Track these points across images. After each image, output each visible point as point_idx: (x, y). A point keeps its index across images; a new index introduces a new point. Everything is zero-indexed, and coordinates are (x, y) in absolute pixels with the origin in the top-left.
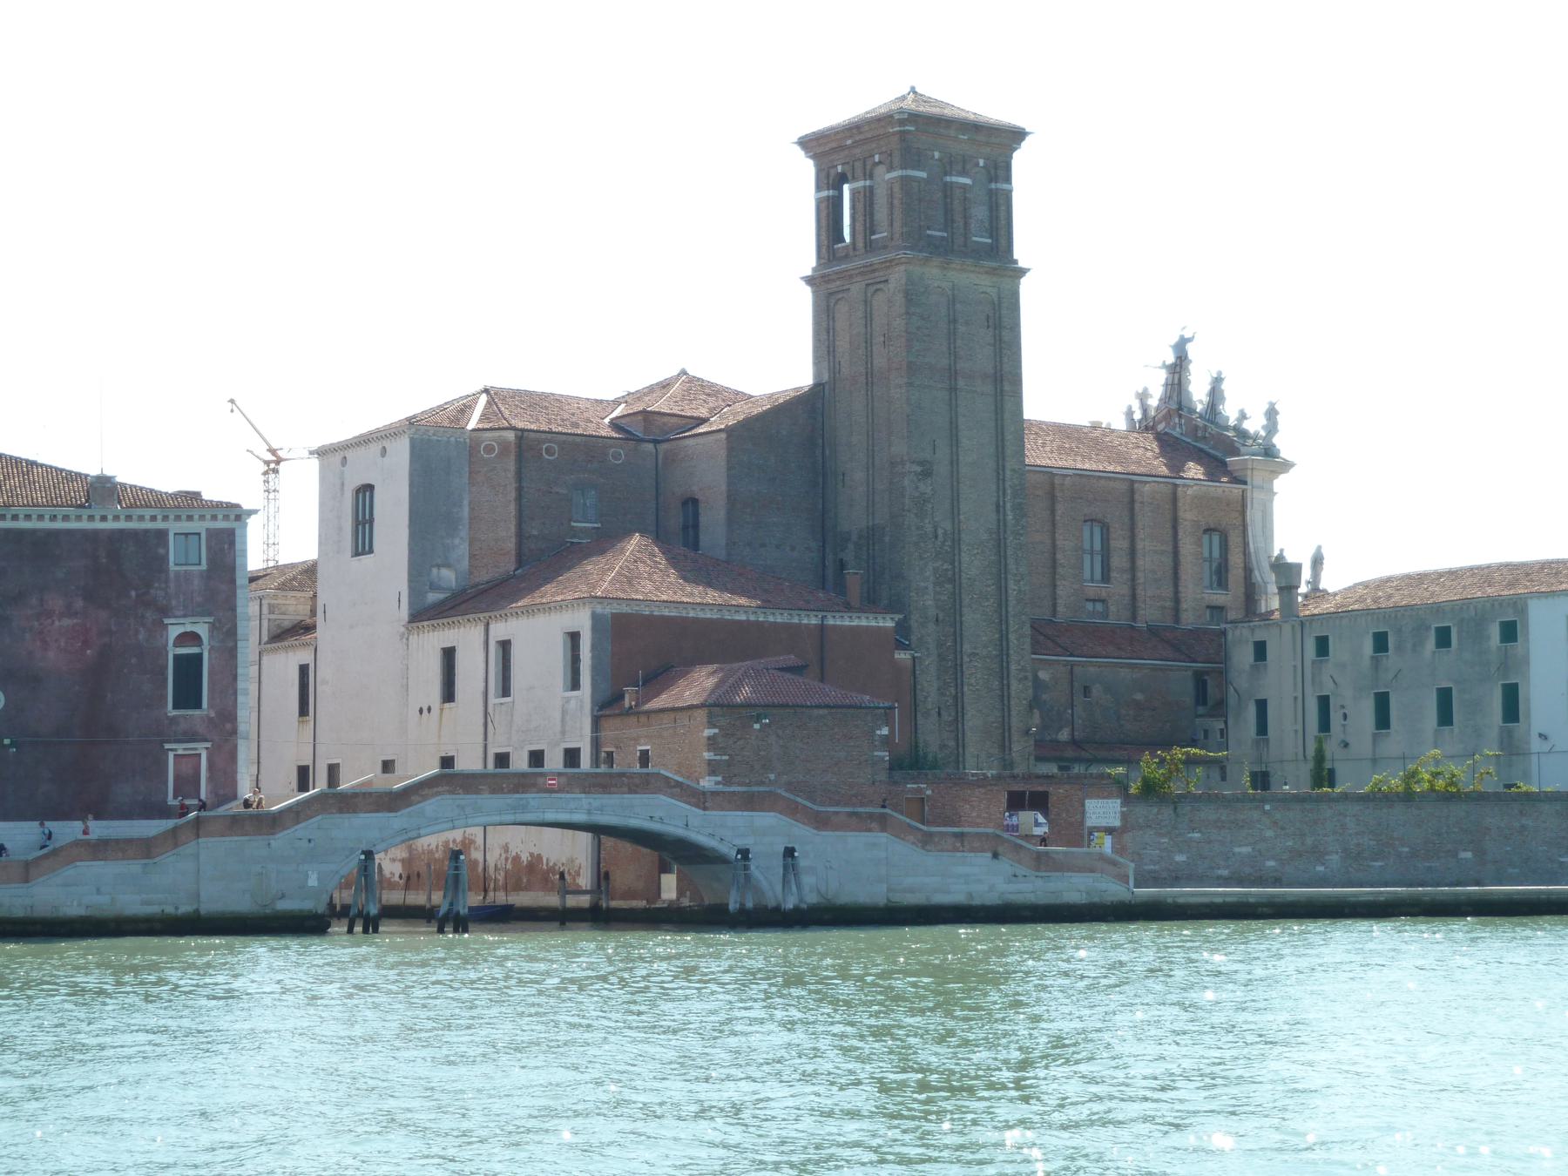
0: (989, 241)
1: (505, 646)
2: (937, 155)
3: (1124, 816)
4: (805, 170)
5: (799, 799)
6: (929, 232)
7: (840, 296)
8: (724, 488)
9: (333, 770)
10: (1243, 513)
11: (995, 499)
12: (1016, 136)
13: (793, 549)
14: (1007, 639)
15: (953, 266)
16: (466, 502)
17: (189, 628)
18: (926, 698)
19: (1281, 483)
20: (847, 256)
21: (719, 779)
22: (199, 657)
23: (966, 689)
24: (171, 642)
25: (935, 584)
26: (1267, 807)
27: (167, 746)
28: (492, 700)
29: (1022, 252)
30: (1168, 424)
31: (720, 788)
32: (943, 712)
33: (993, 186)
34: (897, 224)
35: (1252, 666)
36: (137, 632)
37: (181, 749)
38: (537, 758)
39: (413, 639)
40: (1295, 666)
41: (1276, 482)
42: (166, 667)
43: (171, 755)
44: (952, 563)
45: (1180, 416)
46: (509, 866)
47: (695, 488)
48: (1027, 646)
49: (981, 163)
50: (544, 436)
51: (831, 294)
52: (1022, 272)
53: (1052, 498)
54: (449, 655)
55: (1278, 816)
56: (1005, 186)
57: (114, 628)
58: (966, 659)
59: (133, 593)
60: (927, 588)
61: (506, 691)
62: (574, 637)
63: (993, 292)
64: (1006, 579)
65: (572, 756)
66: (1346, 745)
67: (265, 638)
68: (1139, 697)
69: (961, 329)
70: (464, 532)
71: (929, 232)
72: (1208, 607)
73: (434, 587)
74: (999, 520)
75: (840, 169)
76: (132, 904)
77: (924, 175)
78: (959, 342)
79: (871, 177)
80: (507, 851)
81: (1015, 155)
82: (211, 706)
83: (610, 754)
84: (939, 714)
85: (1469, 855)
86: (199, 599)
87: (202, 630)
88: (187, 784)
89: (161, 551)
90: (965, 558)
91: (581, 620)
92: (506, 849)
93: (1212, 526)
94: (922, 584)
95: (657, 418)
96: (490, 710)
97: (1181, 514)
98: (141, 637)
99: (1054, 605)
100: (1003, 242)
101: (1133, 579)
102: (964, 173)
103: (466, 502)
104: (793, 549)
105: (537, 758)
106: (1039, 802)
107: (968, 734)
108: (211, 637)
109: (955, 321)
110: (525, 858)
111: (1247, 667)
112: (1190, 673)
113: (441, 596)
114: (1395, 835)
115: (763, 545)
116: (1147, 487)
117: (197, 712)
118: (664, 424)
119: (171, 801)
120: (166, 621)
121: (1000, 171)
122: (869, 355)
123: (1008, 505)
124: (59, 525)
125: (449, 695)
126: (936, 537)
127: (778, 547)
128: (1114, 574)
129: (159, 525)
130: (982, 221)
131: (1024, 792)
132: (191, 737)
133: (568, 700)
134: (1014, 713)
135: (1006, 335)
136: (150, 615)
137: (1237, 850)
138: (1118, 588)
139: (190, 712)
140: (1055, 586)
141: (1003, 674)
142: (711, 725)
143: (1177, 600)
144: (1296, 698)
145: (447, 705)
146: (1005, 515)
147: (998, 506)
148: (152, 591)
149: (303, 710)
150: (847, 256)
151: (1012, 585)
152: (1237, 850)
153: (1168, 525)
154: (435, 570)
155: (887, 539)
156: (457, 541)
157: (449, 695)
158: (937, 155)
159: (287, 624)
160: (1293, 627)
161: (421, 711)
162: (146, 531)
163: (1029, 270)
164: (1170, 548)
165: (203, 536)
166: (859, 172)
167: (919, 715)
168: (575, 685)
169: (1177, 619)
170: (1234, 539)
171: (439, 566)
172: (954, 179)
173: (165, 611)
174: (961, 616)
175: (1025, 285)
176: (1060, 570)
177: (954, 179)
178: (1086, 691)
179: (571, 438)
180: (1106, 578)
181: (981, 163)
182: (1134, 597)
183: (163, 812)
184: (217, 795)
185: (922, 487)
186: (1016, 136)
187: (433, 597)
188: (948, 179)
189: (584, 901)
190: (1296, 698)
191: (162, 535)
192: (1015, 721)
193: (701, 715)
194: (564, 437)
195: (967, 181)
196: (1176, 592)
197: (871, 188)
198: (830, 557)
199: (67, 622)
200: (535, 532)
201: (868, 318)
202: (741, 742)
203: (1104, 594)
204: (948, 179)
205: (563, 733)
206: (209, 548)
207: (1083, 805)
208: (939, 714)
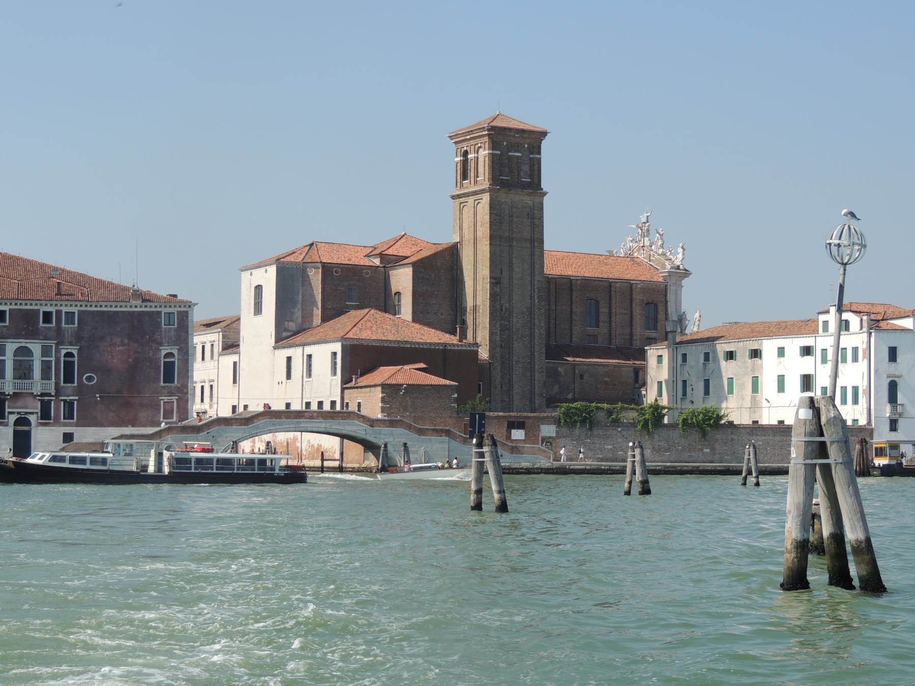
1: (310, 356)
2: (505, 143)
3: (557, 432)
5: (412, 424)
6: (501, 177)
7: (465, 204)
8: (411, 288)
10: (666, 295)
11: (530, 294)
12: (544, 134)
13: (442, 314)
14: (534, 355)
15: (512, 192)
16: (300, 294)
17: (169, 351)
18: (495, 380)
19: (685, 282)
20: (467, 187)
21: (386, 414)
22: (174, 362)
23: (514, 376)
24: (162, 356)
25: (501, 331)
26: (619, 429)
27: (160, 398)
28: (305, 379)
29: (544, 185)
30: (639, 253)
31: (386, 418)
32: (503, 386)
33: (531, 156)
34: (487, 174)
35: (657, 366)
36: (149, 352)
37: (166, 399)
38: (320, 404)
39: (277, 351)
40: (673, 367)
41: (683, 281)
42: (160, 366)
43: (162, 402)
44: (509, 322)
45: (644, 250)
46: (310, 449)
47: (400, 288)
48: (544, 358)
49: (526, 146)
50: (334, 265)
51: (461, 203)
52: (545, 194)
53: (571, 290)
54: (289, 359)
55: (624, 433)
56: (538, 156)
57: (140, 351)
58: (514, 363)
59: (148, 337)
60: (496, 333)
61: (309, 374)
62: (335, 354)
63: (530, 203)
64: (534, 328)
65: (333, 403)
66: (693, 402)
67: (221, 350)
68: (606, 379)
69: (515, 219)
70: (299, 306)
71: (501, 177)
72: (647, 338)
73: (286, 330)
74: (531, 303)
75: (465, 148)
78: (514, 225)
79: (478, 153)
80: (309, 443)
81: (543, 142)
82: (178, 382)
83: (347, 403)
84: (502, 387)
85: (708, 450)
86: (174, 339)
87: (175, 352)
89: (159, 320)
90: (515, 320)
91: (337, 347)
92: (309, 442)
93: (650, 301)
94: (494, 331)
95: (385, 256)
96: (304, 384)
97: (634, 296)
98: (150, 354)
99: (571, 338)
100: (536, 181)
101: (610, 326)
103: (300, 294)
104: (442, 314)
105: (320, 404)
106: (520, 425)
107: (515, 396)
108: (179, 354)
109: (513, 216)
110: (316, 446)
111: (655, 367)
112: (632, 369)
114: (676, 441)
115: (429, 313)
116: (618, 284)
117: (173, 385)
118: (390, 259)
120: (160, 348)
122: (475, 231)
123: (536, 296)
124: (118, 309)
125: (289, 376)
126: (502, 310)
127: (435, 314)
128: (601, 324)
129: (158, 309)
130: (526, 172)
131: (514, 422)
132: (171, 394)
134: (536, 387)
135: (536, 221)
136: (154, 345)
137: (606, 447)
138: (603, 329)
139: (170, 385)
140: (571, 329)
141: (532, 370)
143: (631, 335)
144: (673, 381)
145: (288, 381)
146: (534, 300)
147: (531, 297)
148: (155, 336)
149: (235, 382)
150: (467, 187)
151: (537, 331)
152: (606, 447)
153: (628, 301)
154: (286, 323)
155: (481, 311)
156: (296, 310)
157: (289, 376)
158: (505, 143)
159: (230, 343)
160: (673, 349)
161: (279, 383)
162: (153, 312)
164: (629, 312)
165: (176, 314)
166: (472, 150)
167: (492, 388)
168: (335, 374)
169: (631, 344)
170: (661, 308)
171: (288, 321)
172: (513, 154)
173: (160, 344)
174: (513, 345)
176: (574, 322)
177: (513, 154)
178: (582, 377)
179: (347, 266)
180: (597, 326)
181: (526, 146)
182: (610, 334)
184: (180, 418)
185: (495, 288)
186: (544, 134)
187: (285, 334)
188: (510, 154)
189: (336, 464)
190: (673, 381)
191: (159, 313)
192: (537, 390)
193: (379, 389)
194: (343, 266)
195: (519, 154)
196: (631, 332)
197: (478, 158)
198: (459, 318)
199: (121, 348)
200: (330, 307)
201: (475, 214)
202: (395, 399)
203: (596, 333)
204: (510, 154)
205: (330, 394)
206: (178, 319)
207: (539, 427)
208: (502, 387)
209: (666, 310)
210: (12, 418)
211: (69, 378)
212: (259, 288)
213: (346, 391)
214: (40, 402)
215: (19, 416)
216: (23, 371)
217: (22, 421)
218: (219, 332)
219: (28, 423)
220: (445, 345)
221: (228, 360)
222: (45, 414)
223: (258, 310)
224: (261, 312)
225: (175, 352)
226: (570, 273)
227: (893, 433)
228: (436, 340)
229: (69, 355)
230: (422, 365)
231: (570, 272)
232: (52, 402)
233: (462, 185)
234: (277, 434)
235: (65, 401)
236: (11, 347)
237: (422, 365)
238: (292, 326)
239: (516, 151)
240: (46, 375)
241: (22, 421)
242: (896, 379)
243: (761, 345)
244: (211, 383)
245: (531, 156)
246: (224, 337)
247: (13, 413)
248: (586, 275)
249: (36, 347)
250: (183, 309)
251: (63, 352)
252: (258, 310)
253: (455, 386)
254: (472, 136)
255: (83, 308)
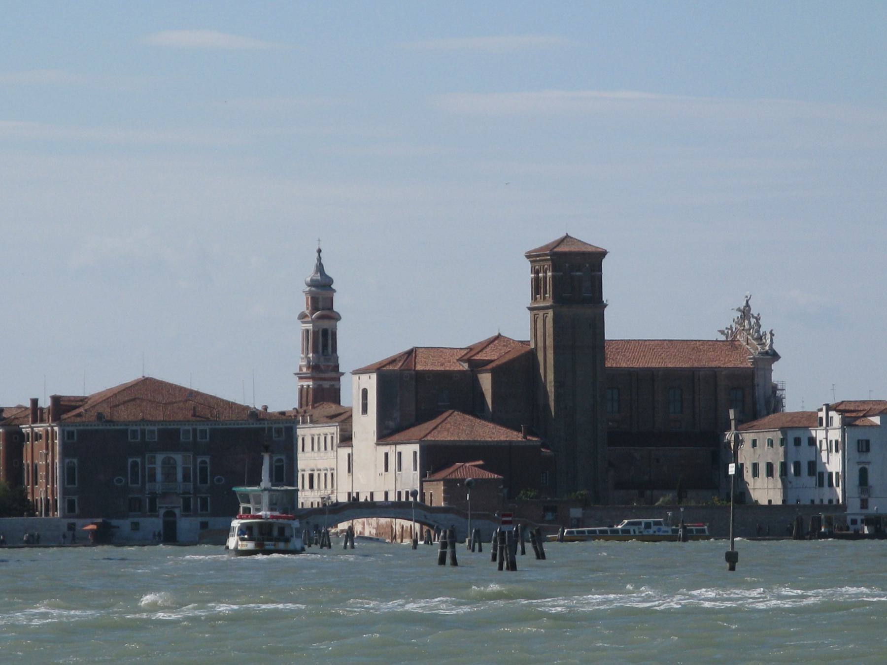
0: (591, 295)
1: (400, 454)
2: (567, 265)
4: (527, 265)
12: (603, 254)
17: (279, 457)
22: (283, 465)
28: (397, 473)
33: (593, 274)
49: (587, 265)
52: (606, 306)
54: (386, 455)
61: (400, 470)
62: (415, 453)
67: (338, 442)
77: (561, 274)
81: (603, 260)
91: (416, 447)
125: (386, 470)
145: (386, 473)
149: (349, 471)
157: (386, 470)
158: (567, 265)
161: (380, 474)
181: (587, 265)
186: (603, 254)
187: (386, 432)
209: (754, 393)
210: (162, 512)
211: (204, 480)
212: (365, 392)
213: (424, 483)
214: (182, 500)
215: (167, 509)
216: (169, 475)
217: (170, 514)
219: (174, 515)
220: (510, 442)
222: (186, 508)
223: (365, 410)
225: (283, 457)
226: (654, 365)
228: (503, 438)
229: (204, 462)
230: (481, 462)
231: (654, 364)
232: (191, 499)
233: (536, 299)
234: (379, 518)
235: (201, 498)
236: (160, 457)
237: (481, 462)
238: (392, 424)
239: (577, 271)
240: (186, 478)
241: (170, 514)
242: (867, 466)
247: (163, 507)
248: (670, 365)
249: (178, 457)
250: (288, 425)
251: (199, 460)
252: (365, 410)
253: (501, 479)
255: (214, 427)
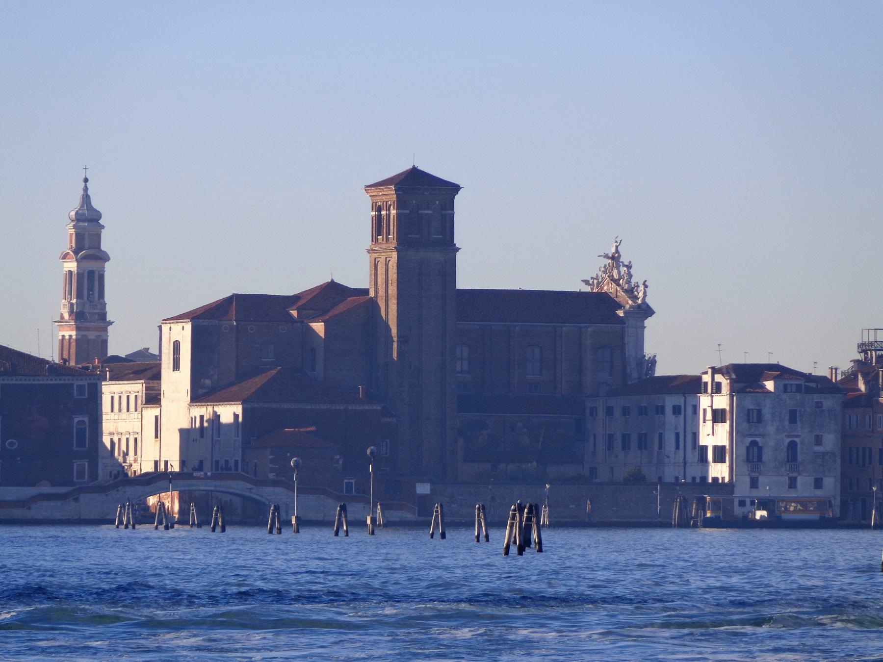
0: (441, 237)
3: (431, 490)
9: (166, 462)
10: (622, 337)
12: (456, 188)
19: (648, 322)
24: (75, 425)
27: (73, 461)
28: (215, 438)
29: (458, 242)
38: (227, 461)
42: (73, 433)
43: (75, 464)
49: (437, 202)
56: (451, 212)
76: (58, 515)
77: (407, 212)
81: (456, 197)
85: (574, 506)
88: (81, 474)
102: (428, 209)
113: (205, 391)
119: (75, 480)
120: (73, 416)
121: (450, 205)
129: (71, 382)
133: (235, 441)
142: (272, 454)
145: (202, 439)
149: (156, 437)
163: (460, 249)
172: (423, 212)
175: (459, 255)
177: (423, 212)
181: (437, 202)
183: (72, 483)
186: (456, 188)
187: (201, 391)
188: (420, 212)
191: (73, 384)
195: (430, 212)
204: (420, 212)
212: (177, 346)
218: (142, 383)
221: (151, 413)
223: (176, 366)
224: (179, 368)
227: (753, 490)
233: (377, 240)
239: (425, 209)
243: (664, 401)
244: (136, 436)
245: (443, 212)
246: (147, 389)
252: (176, 366)
254: (384, 193)
